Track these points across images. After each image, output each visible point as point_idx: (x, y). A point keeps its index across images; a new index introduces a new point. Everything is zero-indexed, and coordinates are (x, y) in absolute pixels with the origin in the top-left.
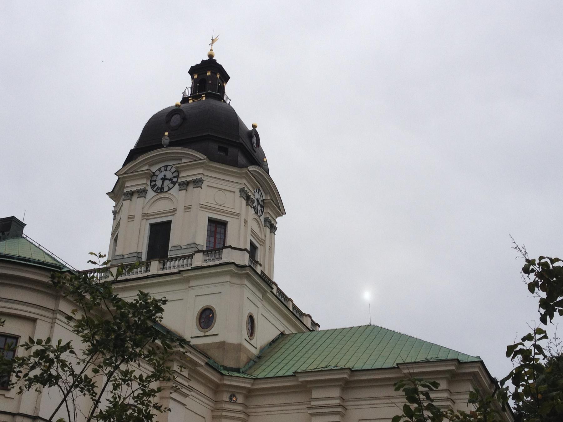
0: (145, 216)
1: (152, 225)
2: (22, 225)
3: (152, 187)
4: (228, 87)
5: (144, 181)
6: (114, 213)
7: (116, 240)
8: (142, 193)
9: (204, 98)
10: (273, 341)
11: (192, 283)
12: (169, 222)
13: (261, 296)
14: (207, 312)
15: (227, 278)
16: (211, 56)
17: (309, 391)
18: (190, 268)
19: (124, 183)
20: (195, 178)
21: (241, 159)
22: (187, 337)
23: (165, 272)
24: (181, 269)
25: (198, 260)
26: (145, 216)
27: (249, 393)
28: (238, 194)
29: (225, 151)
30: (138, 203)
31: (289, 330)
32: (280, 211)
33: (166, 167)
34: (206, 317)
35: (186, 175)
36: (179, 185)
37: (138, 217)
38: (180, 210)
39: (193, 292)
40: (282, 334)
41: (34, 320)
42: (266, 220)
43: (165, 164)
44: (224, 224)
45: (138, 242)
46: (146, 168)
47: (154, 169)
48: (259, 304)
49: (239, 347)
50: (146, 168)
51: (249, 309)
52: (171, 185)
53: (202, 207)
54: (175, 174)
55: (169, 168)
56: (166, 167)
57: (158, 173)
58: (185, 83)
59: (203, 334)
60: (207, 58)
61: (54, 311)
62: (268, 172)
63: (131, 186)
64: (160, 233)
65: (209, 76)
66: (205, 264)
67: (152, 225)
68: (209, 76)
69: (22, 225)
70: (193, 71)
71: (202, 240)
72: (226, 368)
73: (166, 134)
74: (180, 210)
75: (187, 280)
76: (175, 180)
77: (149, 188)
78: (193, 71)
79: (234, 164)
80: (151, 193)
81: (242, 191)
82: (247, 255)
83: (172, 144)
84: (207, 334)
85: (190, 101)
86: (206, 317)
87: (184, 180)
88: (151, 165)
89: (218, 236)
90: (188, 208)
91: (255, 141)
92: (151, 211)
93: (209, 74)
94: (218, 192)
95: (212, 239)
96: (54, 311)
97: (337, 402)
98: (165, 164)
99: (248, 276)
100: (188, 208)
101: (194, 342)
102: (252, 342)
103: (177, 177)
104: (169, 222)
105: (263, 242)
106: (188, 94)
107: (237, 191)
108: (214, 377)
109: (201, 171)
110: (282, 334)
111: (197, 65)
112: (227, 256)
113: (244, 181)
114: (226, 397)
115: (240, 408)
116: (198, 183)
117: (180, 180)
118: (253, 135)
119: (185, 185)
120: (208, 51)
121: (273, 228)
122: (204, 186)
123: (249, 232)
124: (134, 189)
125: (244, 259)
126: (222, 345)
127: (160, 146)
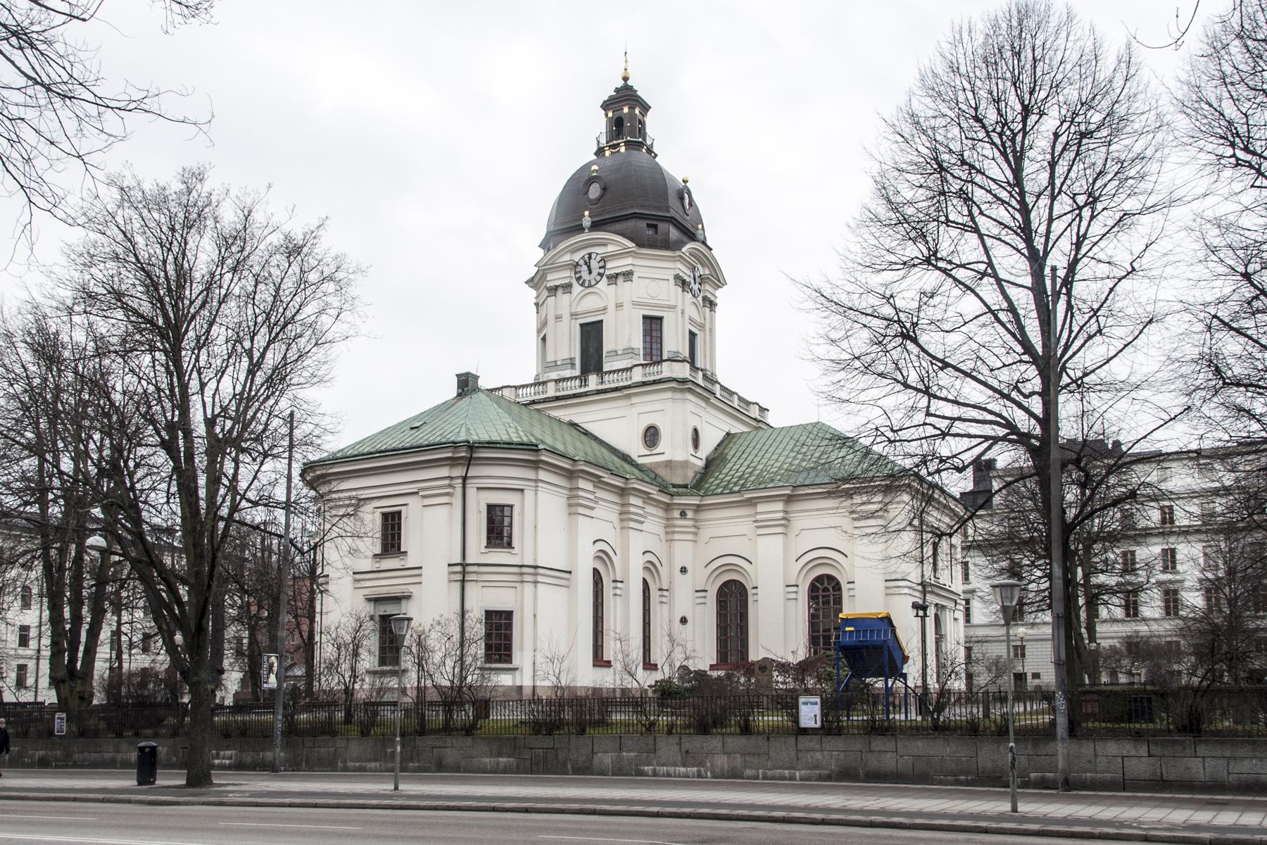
0: (574, 315)
1: (582, 325)
2: (477, 377)
3: (578, 279)
4: (650, 120)
5: (567, 273)
6: (537, 304)
7: (544, 339)
8: (567, 287)
9: (623, 149)
10: (722, 442)
11: (634, 400)
12: (601, 321)
13: (703, 404)
15: (669, 395)
16: (625, 79)
17: (755, 505)
20: (624, 269)
21: (674, 233)
22: (634, 457)
24: (621, 384)
25: (638, 375)
26: (574, 315)
27: (698, 508)
28: (672, 281)
29: (655, 227)
30: (563, 299)
31: (737, 428)
33: (590, 255)
34: (651, 436)
35: (614, 266)
37: (566, 317)
38: (611, 308)
39: (636, 410)
41: (522, 490)
42: (705, 299)
44: (661, 319)
48: (702, 413)
49: (685, 464)
51: (694, 422)
53: (636, 304)
54: (602, 264)
55: (593, 256)
56: (590, 255)
58: (599, 124)
60: (620, 83)
61: (536, 481)
62: (704, 243)
63: (555, 278)
64: (592, 334)
66: (645, 379)
67: (582, 325)
69: (477, 377)
71: (638, 342)
72: (674, 486)
73: (587, 213)
74: (611, 308)
75: (629, 396)
76: (602, 271)
77: (574, 282)
78: (606, 106)
79: (666, 245)
80: (577, 288)
81: (677, 277)
82: (688, 366)
83: (596, 226)
85: (607, 153)
87: (612, 272)
88: (573, 252)
89: (654, 334)
90: (619, 306)
91: (687, 201)
92: (579, 309)
93: (626, 110)
94: (652, 280)
95: (648, 339)
96: (536, 481)
98: (590, 250)
99: (690, 390)
100: (619, 306)
101: (640, 461)
103: (603, 267)
104: (601, 321)
105: (702, 327)
106: (603, 141)
108: (665, 499)
109: (629, 261)
111: (611, 98)
112: (667, 370)
113: (679, 265)
114: (676, 514)
115: (691, 523)
116: (628, 275)
117: (608, 273)
118: (683, 194)
119: (613, 278)
120: (621, 73)
122: (635, 277)
123: (687, 321)
124: (557, 283)
125: (682, 371)
126: (669, 464)
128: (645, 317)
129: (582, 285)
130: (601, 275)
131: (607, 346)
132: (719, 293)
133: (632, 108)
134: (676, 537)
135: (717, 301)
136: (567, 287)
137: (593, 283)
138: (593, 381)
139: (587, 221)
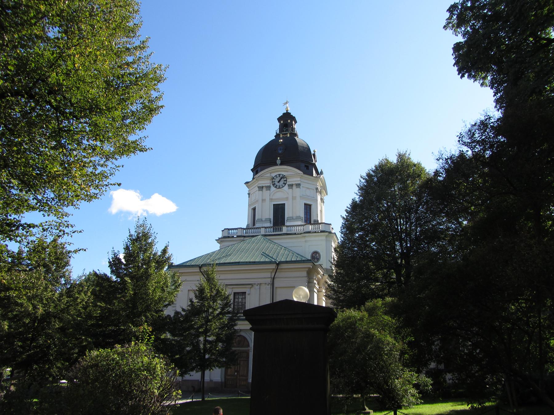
0: (271, 200)
1: (274, 205)
3: (274, 185)
6: (249, 194)
8: (268, 188)
16: (287, 111)
20: (297, 183)
30: (266, 193)
36: (289, 185)
43: (279, 173)
44: (310, 205)
45: (267, 213)
46: (269, 175)
50: (269, 175)
52: (284, 185)
57: (275, 178)
60: (285, 112)
65: (287, 121)
67: (274, 205)
68: (287, 121)
70: (279, 119)
77: (272, 185)
78: (279, 119)
80: (273, 188)
100: (294, 198)
116: (298, 185)
122: (301, 187)
124: (264, 185)
127: (276, 164)
128: (305, 204)
129: (276, 187)
131: (287, 214)
136: (268, 188)
137: (281, 187)
139: (278, 162)
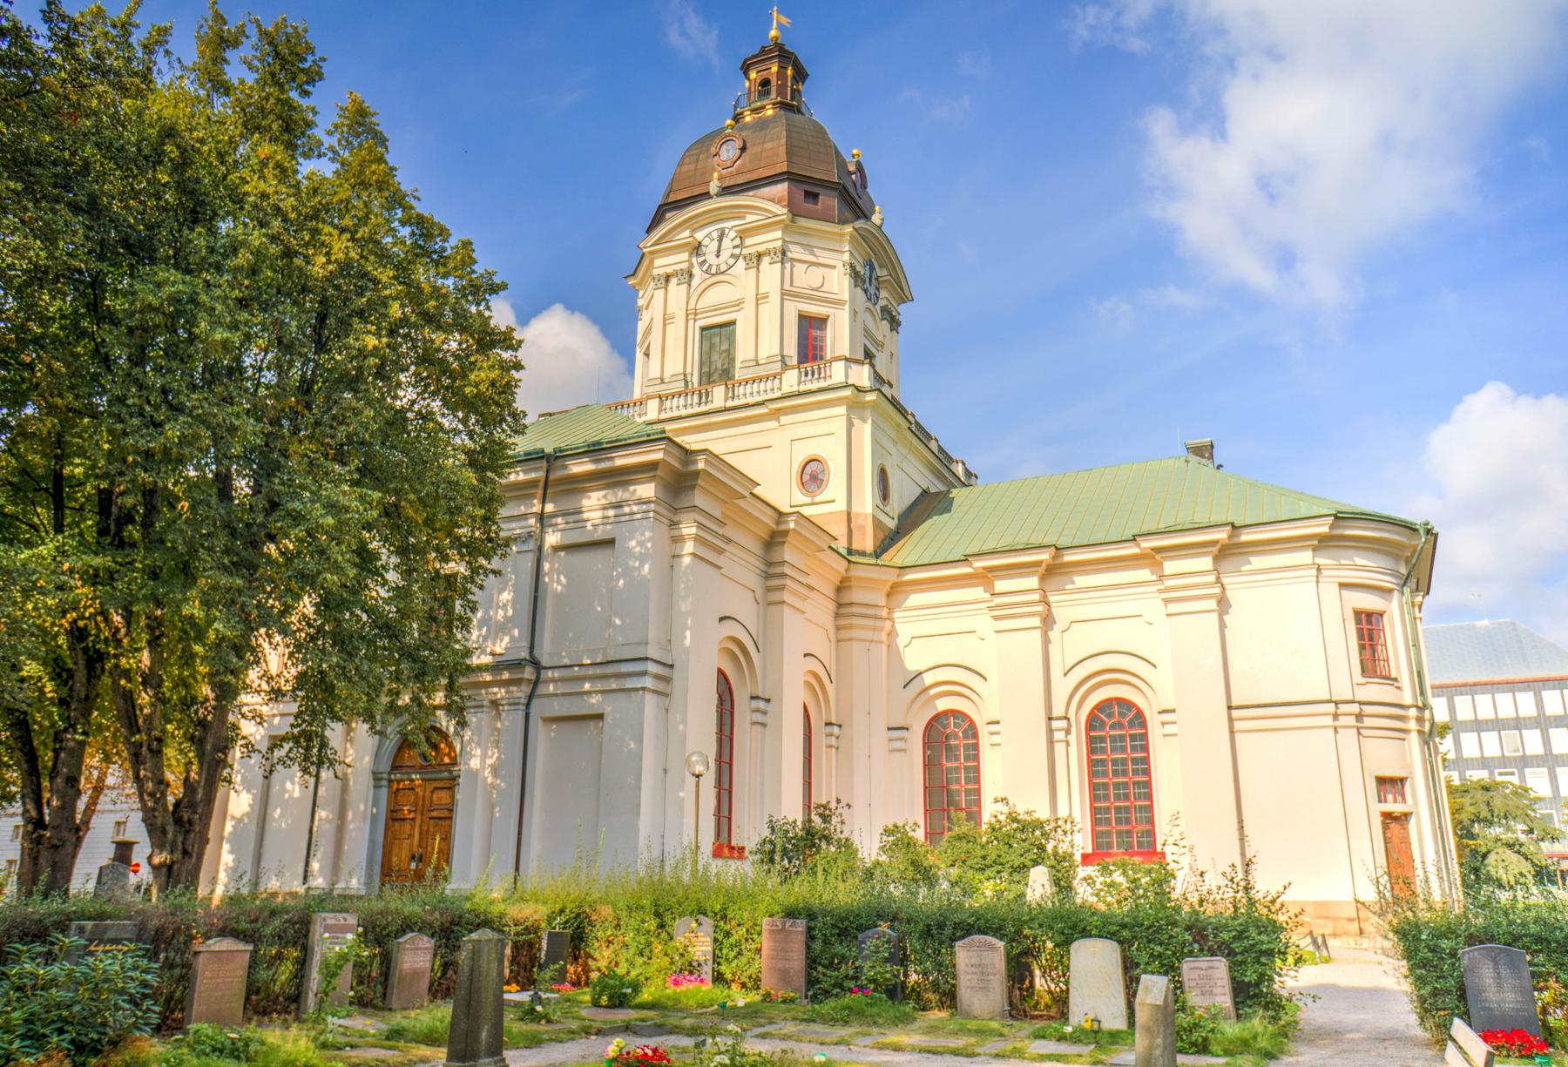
0: (692, 314)
1: (703, 329)
12: (733, 323)
14: (813, 466)
18: (778, 394)
19: (652, 262)
23: (736, 402)
25: (790, 381)
32: (904, 297)
35: (756, 243)
40: (925, 492)
42: (884, 309)
46: (687, 233)
47: (699, 236)
52: (731, 261)
54: (737, 241)
59: (808, 500)
76: (737, 251)
83: (726, 191)
84: (817, 499)
86: (812, 475)
87: (752, 250)
97: (1036, 597)
102: (887, 509)
104: (733, 323)
107: (839, 264)
110: (925, 492)
117: (745, 252)
121: (895, 324)
127: (706, 196)
130: (736, 257)
131: (743, 352)
132: (901, 308)
133: (782, 68)
134: (855, 633)
135: (901, 318)
138: (718, 395)
139: (714, 187)
